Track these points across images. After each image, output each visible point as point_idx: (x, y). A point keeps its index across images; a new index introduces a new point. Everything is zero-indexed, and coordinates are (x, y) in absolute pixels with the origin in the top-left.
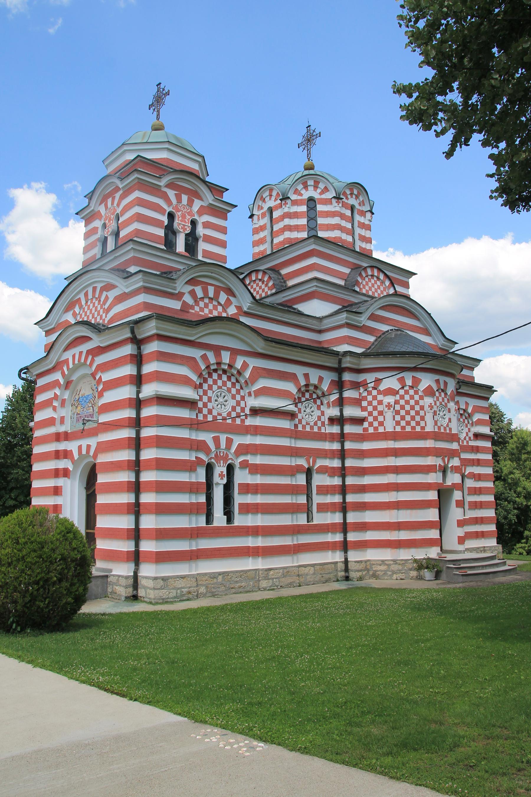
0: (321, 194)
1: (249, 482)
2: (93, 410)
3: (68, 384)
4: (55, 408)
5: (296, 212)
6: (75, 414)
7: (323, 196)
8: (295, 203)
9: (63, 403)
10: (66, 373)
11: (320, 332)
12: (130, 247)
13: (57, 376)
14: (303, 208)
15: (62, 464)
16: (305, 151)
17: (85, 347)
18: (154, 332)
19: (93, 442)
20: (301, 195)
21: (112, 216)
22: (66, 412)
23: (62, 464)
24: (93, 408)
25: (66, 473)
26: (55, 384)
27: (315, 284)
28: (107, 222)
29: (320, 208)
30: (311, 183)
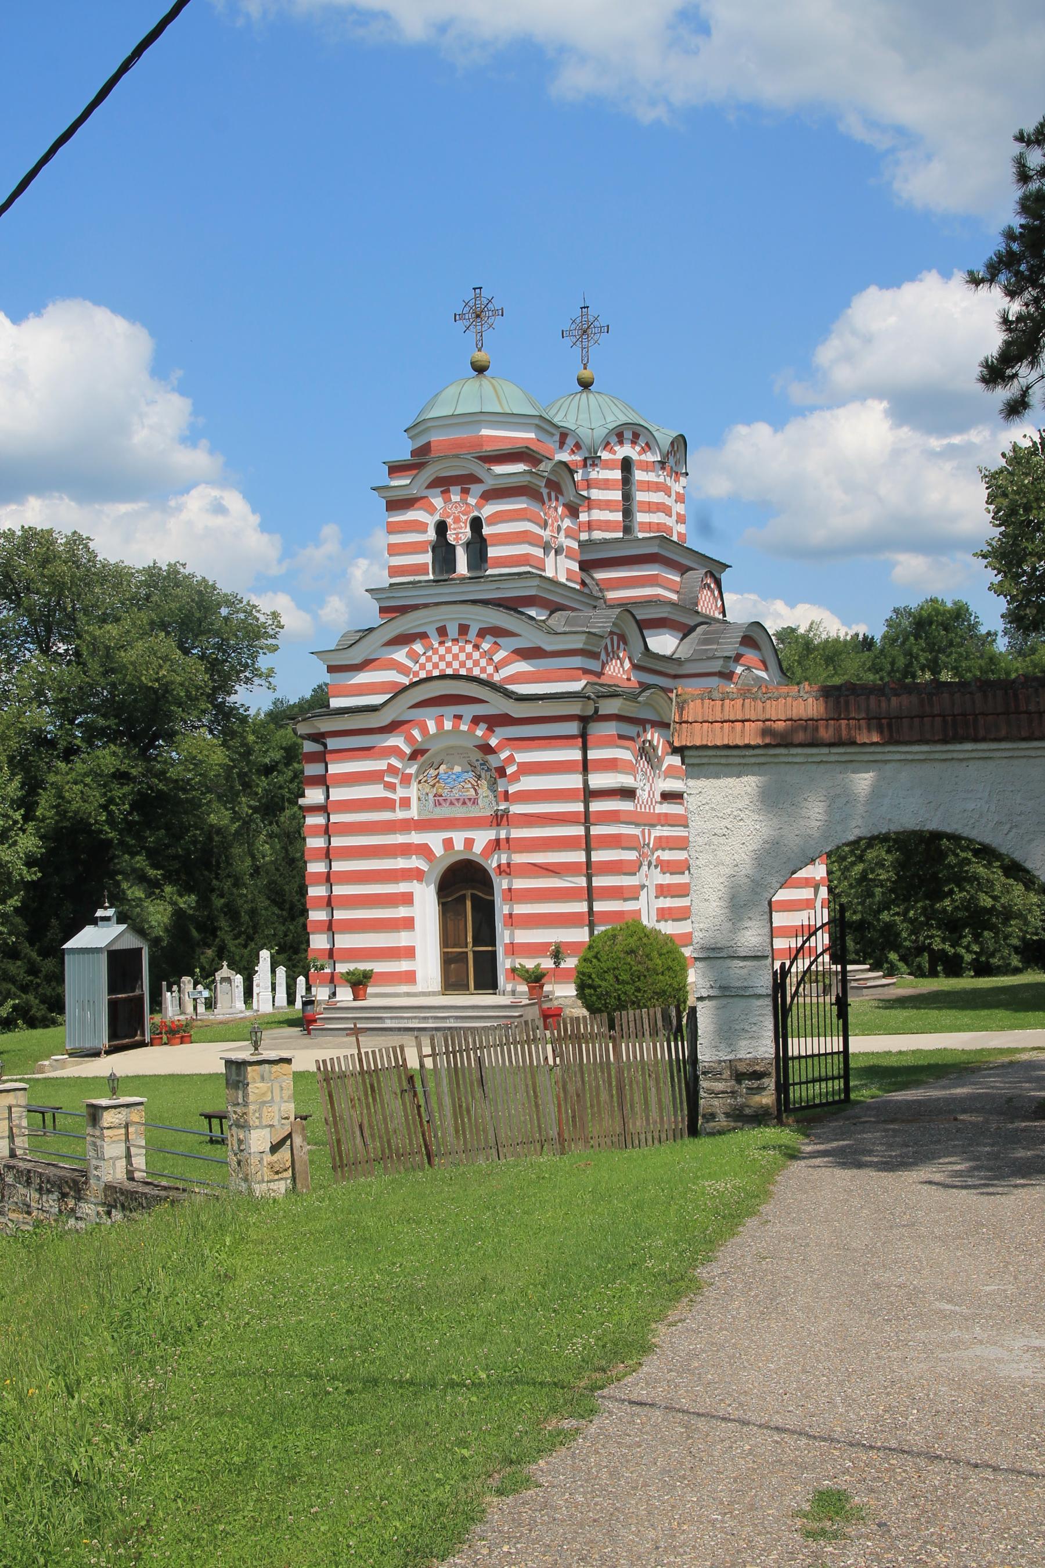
0: (640, 454)
1: (660, 882)
2: (477, 793)
3: (414, 755)
4: (391, 787)
5: (607, 480)
6: (431, 796)
7: (643, 457)
8: (608, 465)
9: (406, 780)
10: (419, 740)
11: (676, 677)
12: (535, 584)
13: (396, 740)
14: (617, 474)
15: (415, 862)
16: (577, 349)
17: (469, 711)
18: (616, 712)
19: (482, 838)
20: (614, 453)
21: (464, 518)
22: (413, 791)
23: (415, 862)
24: (475, 790)
25: (417, 875)
26: (396, 751)
27: (669, 609)
28: (449, 521)
29: (639, 475)
30: (628, 435)
